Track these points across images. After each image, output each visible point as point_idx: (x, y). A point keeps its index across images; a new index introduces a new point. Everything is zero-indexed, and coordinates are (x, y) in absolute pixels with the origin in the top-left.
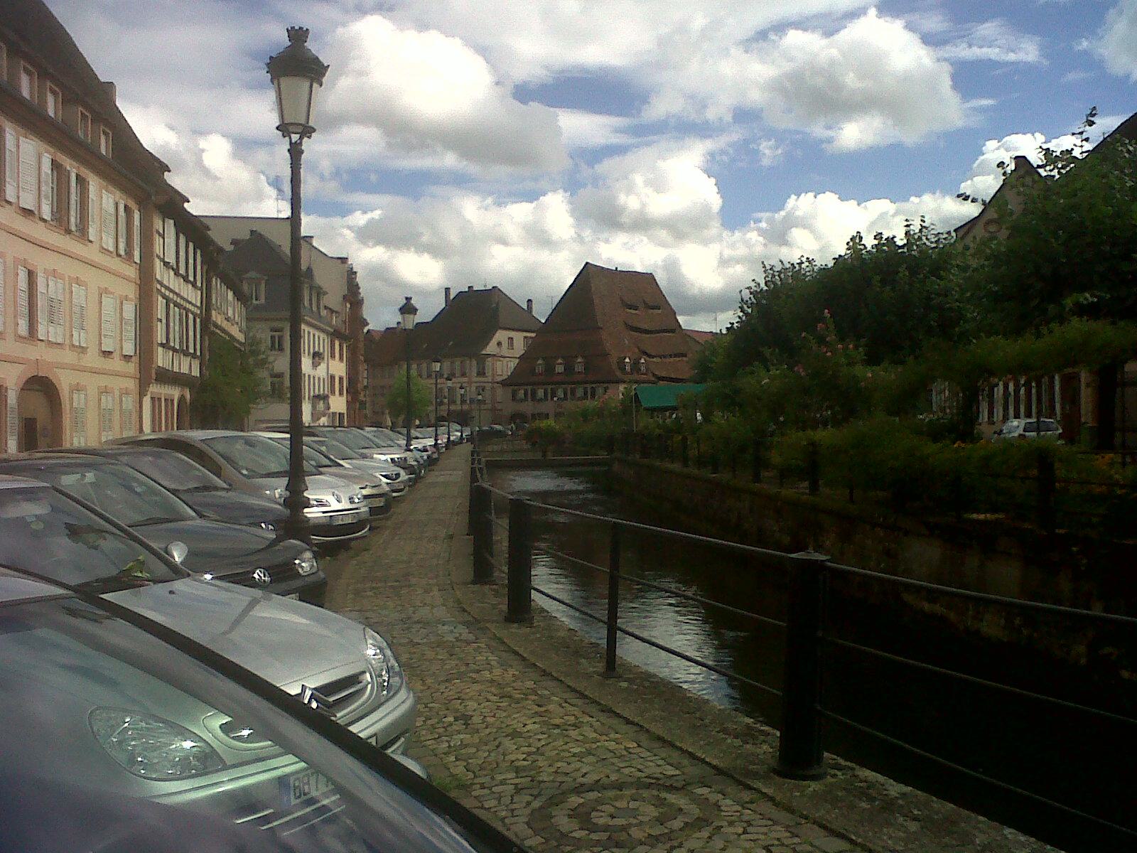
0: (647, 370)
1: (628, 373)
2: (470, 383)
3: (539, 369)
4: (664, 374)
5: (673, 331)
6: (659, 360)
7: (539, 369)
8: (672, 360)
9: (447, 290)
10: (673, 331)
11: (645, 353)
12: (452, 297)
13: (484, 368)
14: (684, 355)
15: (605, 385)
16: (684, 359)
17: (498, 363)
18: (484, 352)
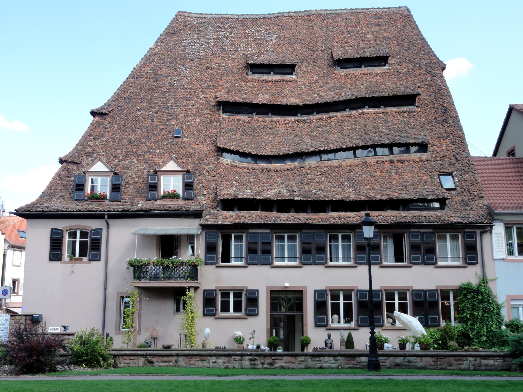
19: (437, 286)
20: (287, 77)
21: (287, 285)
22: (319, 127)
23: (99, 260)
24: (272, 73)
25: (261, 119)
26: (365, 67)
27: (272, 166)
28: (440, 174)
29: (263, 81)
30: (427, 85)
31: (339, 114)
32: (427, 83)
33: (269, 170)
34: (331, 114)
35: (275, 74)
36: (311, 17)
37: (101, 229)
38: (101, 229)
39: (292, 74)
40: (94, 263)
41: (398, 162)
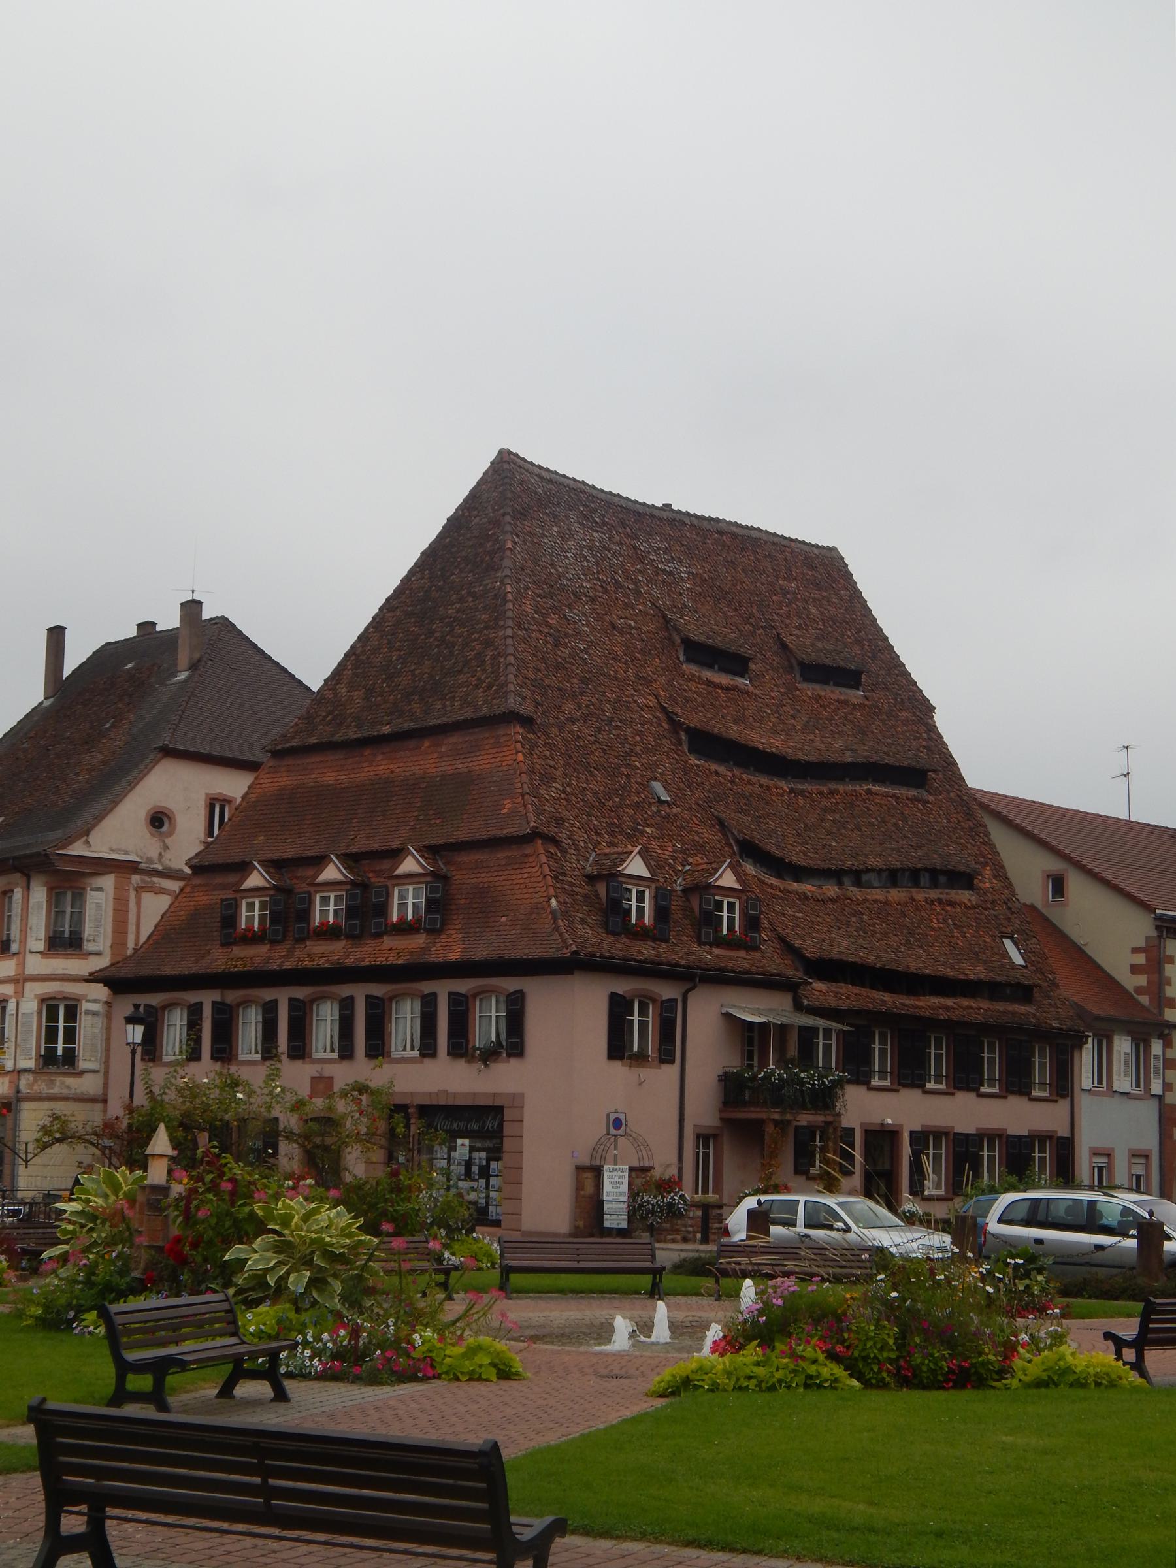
0: (752, 923)
1: (640, 933)
2: (20, 980)
3: (251, 916)
4: (843, 947)
5: (915, 776)
6: (831, 890)
7: (251, 916)
8: (895, 894)
9: (56, 636)
10: (915, 776)
11: (750, 850)
12: (67, 672)
13: (78, 918)
14: (963, 879)
15: (511, 984)
16: (965, 896)
17: (147, 897)
18: (77, 849)
19: (1029, 1131)
20: (743, 682)
21: (889, 1121)
22: (826, 810)
23: (672, 1062)
24: (716, 667)
25: (744, 776)
26: (837, 684)
27: (807, 888)
28: (1002, 937)
29: (709, 683)
30: (924, 747)
31: (841, 788)
32: (924, 743)
33: (807, 898)
34: (833, 786)
35: (722, 670)
36: (724, 538)
37: (676, 1000)
38: (676, 1000)
39: (743, 677)
40: (666, 1068)
41: (948, 905)
